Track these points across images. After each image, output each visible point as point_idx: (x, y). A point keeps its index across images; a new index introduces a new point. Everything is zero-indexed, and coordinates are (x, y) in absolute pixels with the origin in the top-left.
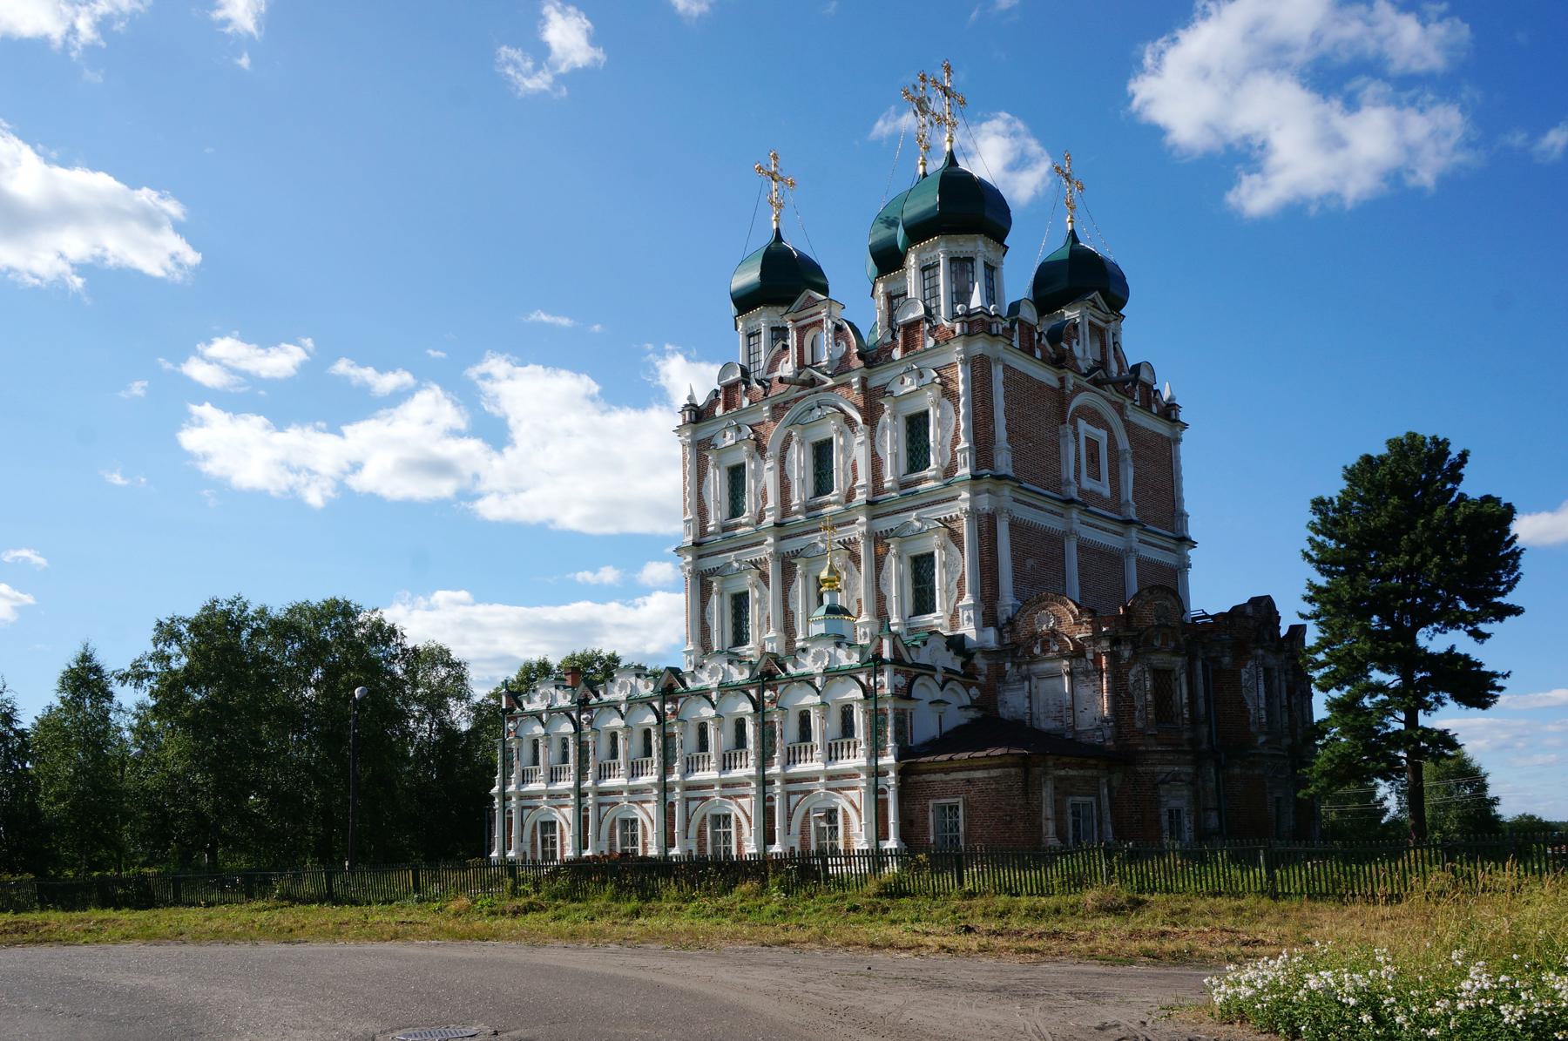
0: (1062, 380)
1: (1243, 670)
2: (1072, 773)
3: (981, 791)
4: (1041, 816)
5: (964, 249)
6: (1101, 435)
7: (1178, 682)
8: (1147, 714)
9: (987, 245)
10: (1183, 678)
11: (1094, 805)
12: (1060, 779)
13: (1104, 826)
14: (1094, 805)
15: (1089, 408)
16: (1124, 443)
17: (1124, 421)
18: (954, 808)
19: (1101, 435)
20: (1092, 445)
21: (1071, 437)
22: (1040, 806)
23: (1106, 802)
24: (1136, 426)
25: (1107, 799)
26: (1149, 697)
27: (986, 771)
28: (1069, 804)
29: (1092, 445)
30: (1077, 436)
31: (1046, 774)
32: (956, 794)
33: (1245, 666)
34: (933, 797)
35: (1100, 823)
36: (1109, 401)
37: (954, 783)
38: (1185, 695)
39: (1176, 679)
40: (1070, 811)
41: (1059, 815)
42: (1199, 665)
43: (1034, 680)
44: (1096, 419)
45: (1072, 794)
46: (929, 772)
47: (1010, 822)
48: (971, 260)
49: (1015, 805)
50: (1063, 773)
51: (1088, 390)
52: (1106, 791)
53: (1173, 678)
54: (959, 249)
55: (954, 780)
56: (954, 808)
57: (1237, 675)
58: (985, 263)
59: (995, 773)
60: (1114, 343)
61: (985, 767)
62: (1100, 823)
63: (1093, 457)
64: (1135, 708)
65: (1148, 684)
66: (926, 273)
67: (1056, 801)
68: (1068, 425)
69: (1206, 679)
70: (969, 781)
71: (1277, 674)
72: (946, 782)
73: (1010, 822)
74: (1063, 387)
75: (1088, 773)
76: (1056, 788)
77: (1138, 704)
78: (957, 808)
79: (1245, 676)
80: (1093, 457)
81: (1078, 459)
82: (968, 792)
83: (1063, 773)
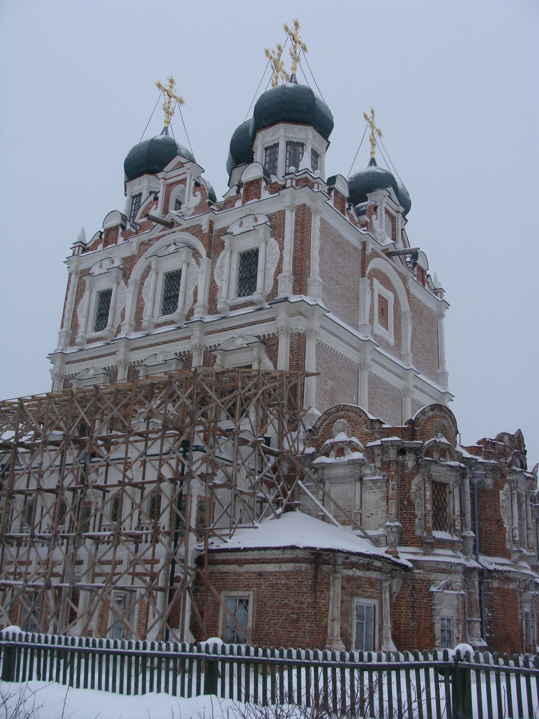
0: (364, 244)
1: (501, 492)
2: (359, 573)
3: (272, 586)
4: (327, 617)
5: (297, 136)
6: (389, 295)
7: (451, 495)
8: (426, 522)
9: (314, 137)
10: (456, 492)
11: (377, 611)
12: (348, 579)
13: (384, 631)
14: (377, 611)
15: (382, 273)
16: (405, 305)
17: (406, 289)
18: (244, 602)
19: (389, 295)
20: (383, 301)
21: (368, 288)
22: (327, 605)
23: (387, 609)
24: (414, 297)
25: (388, 603)
26: (429, 506)
27: (278, 565)
28: (354, 606)
29: (383, 301)
30: (372, 290)
31: (335, 572)
32: (247, 587)
33: (502, 488)
34: (225, 588)
35: (381, 629)
36: (397, 271)
37: (247, 575)
38: (457, 508)
39: (450, 493)
40: (355, 613)
41: (345, 615)
42: (467, 482)
43: (328, 484)
44: (386, 282)
45: (358, 595)
46: (224, 562)
47: (297, 620)
48: (302, 145)
49: (302, 603)
50: (350, 573)
51: (382, 257)
52: (388, 594)
53: (447, 491)
54: (293, 136)
55: (246, 572)
56: (244, 602)
57: (495, 494)
58: (312, 149)
59: (287, 567)
60: (402, 230)
61: (277, 561)
62: (381, 629)
63: (383, 311)
64: (415, 516)
65: (428, 493)
66: (268, 152)
67: (342, 602)
68: (366, 278)
69: (472, 495)
70: (260, 574)
71: (524, 499)
72: (239, 574)
73: (297, 620)
74: (364, 249)
75: (374, 575)
76: (343, 588)
77: (418, 513)
78: (247, 602)
79: (502, 497)
80: (383, 311)
81: (372, 309)
82: (259, 586)
83: (350, 573)
